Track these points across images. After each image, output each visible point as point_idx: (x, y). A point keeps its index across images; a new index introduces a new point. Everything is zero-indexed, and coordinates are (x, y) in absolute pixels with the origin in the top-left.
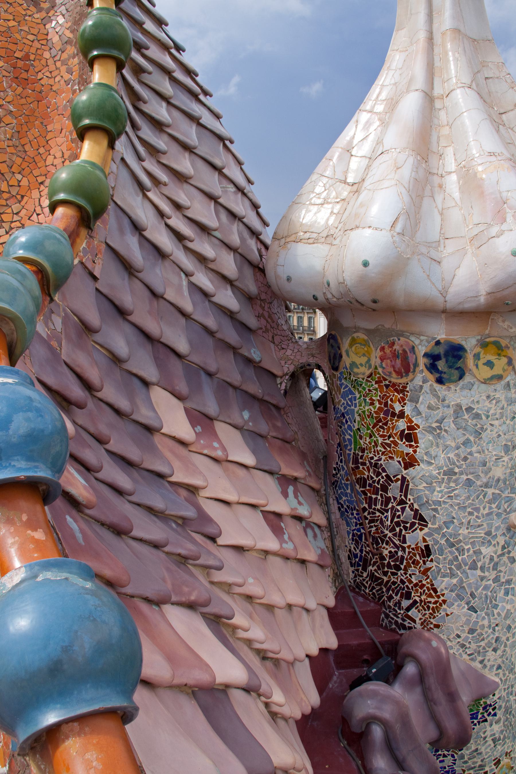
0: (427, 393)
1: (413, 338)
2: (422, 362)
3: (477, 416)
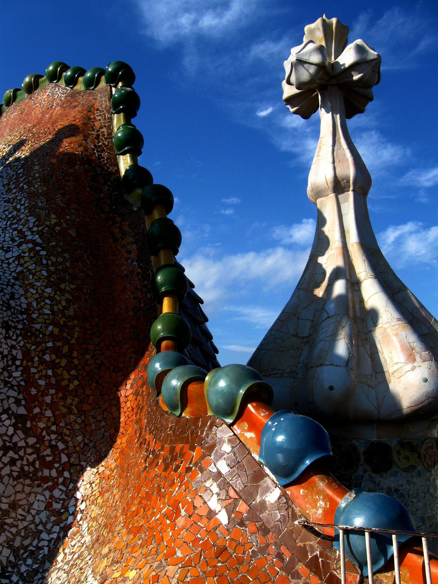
0: (367, 480)
1: (354, 442)
2: (362, 457)
3: (402, 495)
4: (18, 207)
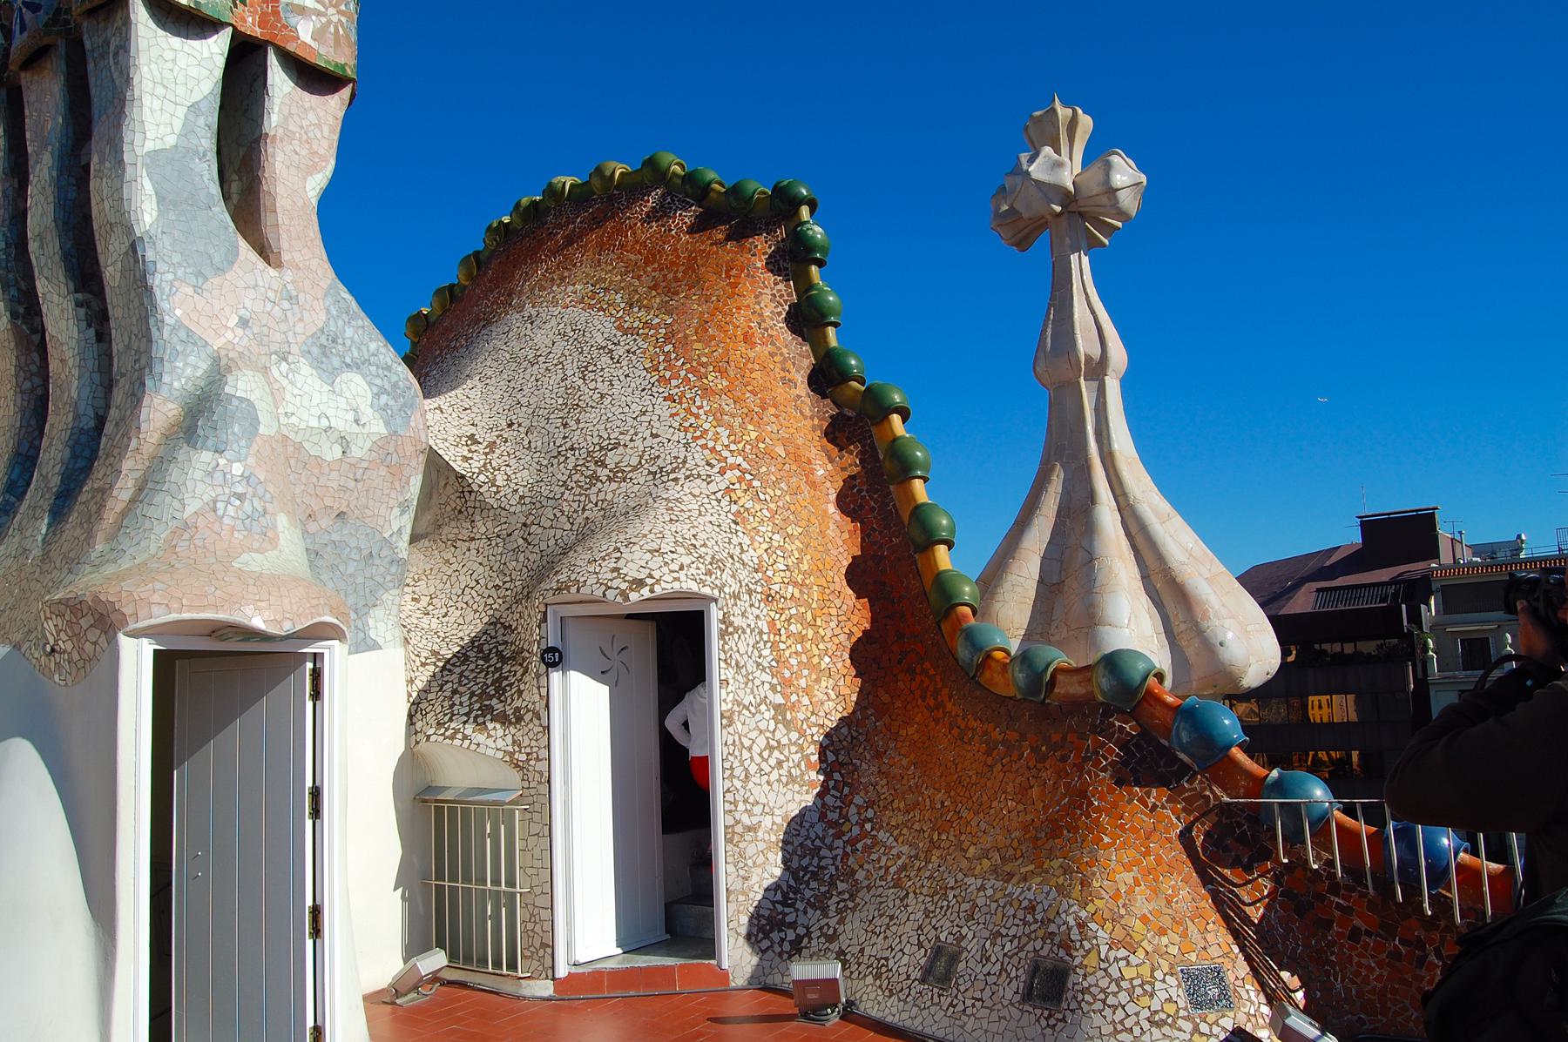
4: (694, 410)
